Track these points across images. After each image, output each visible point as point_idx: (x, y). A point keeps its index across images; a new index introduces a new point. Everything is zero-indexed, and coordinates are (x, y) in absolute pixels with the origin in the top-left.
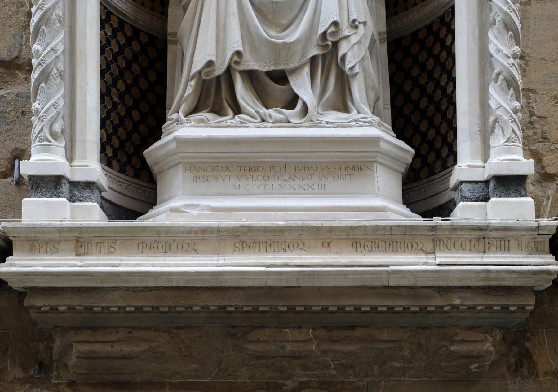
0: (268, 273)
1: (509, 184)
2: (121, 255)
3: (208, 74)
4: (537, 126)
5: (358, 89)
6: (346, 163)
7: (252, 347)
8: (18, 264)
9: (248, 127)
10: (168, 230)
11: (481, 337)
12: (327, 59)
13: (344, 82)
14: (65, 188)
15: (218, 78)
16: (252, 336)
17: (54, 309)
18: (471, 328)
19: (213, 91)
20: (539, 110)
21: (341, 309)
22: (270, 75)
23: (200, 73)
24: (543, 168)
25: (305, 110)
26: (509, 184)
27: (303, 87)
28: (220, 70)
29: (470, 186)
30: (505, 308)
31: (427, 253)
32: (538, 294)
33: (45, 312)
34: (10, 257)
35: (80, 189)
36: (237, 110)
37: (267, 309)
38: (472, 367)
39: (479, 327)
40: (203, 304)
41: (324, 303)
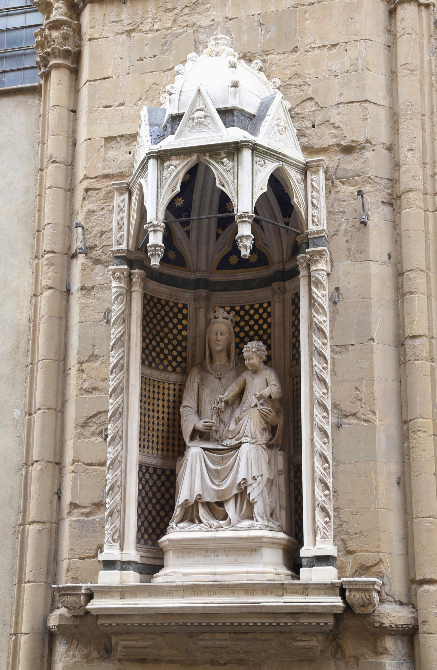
0: (205, 607)
1: (323, 560)
2: (140, 598)
3: (186, 504)
4: (343, 526)
5: (258, 509)
6: (248, 548)
7: (200, 643)
8: (96, 604)
9: (203, 531)
10: (160, 587)
11: (309, 638)
12: (242, 495)
13: (251, 505)
14: (119, 565)
15: (193, 505)
16: (200, 637)
17: (110, 625)
18: (305, 633)
19: (190, 511)
20: (344, 518)
21: (240, 624)
22: (217, 503)
23: (182, 504)
24: (347, 548)
25: (230, 522)
26: (323, 560)
27: (230, 509)
28: (192, 502)
29: (306, 559)
30: (318, 624)
31: (280, 596)
32: (336, 616)
33: (106, 626)
34: (92, 600)
35: (124, 565)
36: (200, 522)
37: (205, 624)
38: (310, 653)
39: (309, 633)
40: (176, 622)
41: (232, 621)
